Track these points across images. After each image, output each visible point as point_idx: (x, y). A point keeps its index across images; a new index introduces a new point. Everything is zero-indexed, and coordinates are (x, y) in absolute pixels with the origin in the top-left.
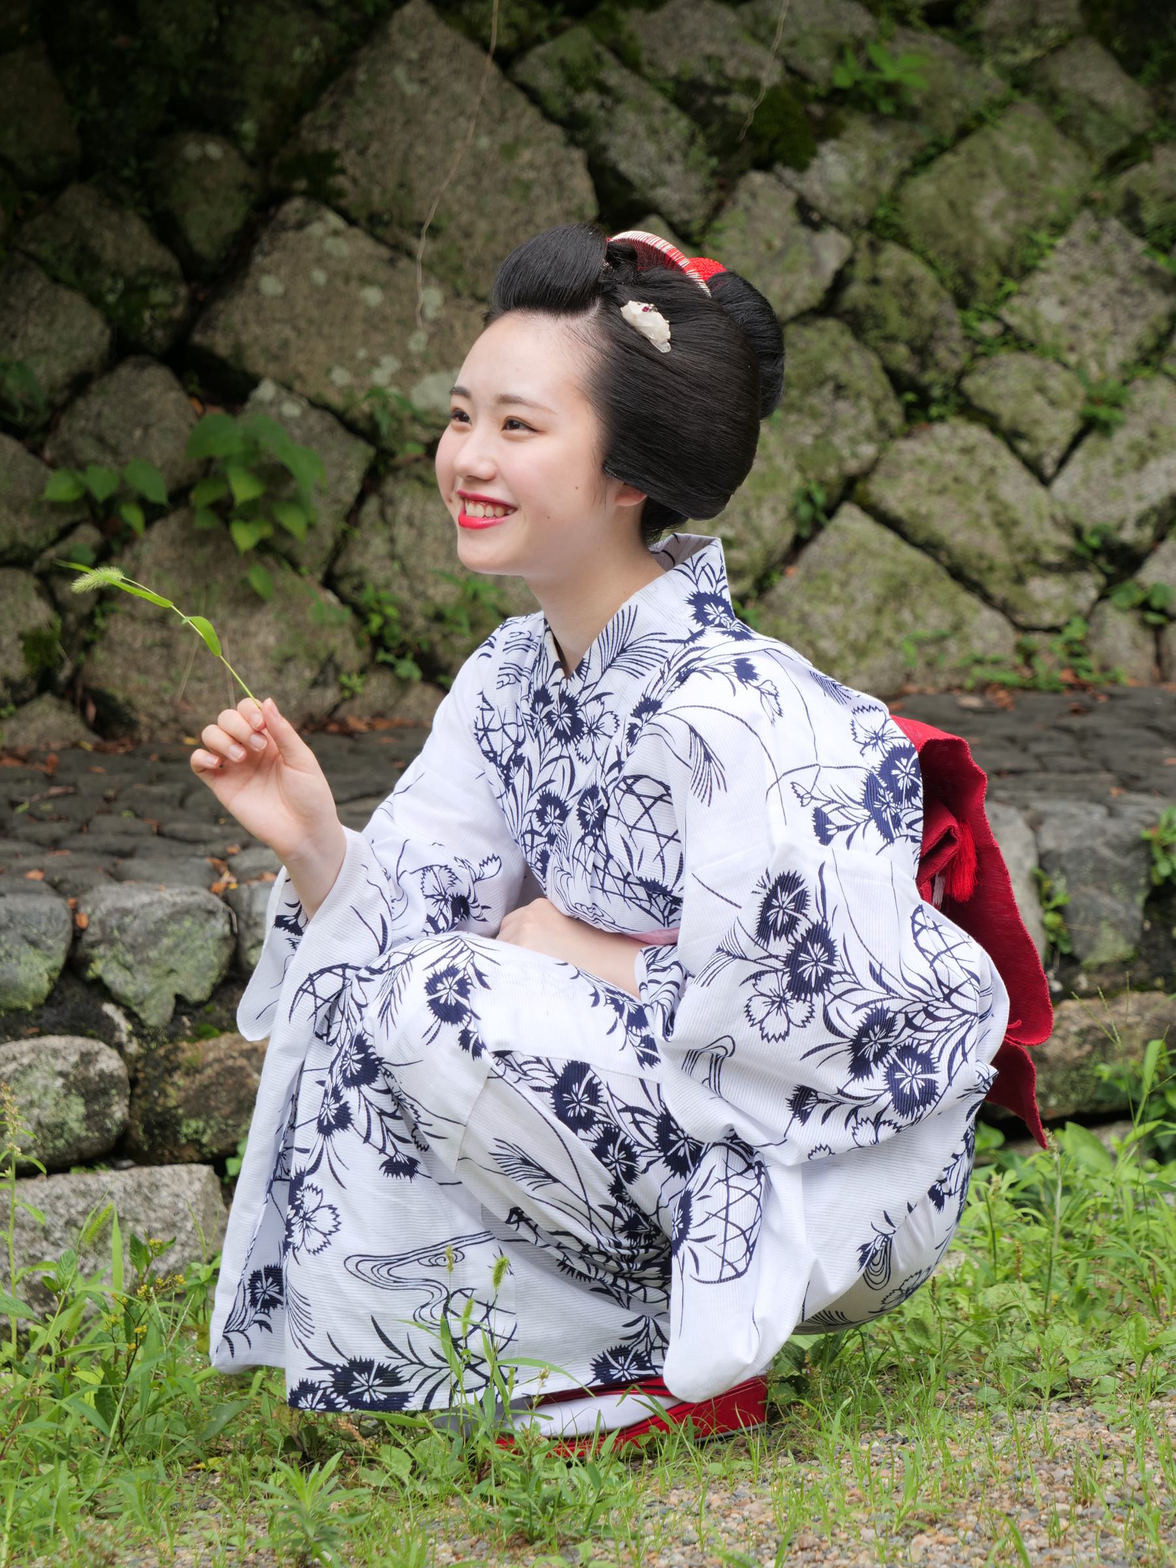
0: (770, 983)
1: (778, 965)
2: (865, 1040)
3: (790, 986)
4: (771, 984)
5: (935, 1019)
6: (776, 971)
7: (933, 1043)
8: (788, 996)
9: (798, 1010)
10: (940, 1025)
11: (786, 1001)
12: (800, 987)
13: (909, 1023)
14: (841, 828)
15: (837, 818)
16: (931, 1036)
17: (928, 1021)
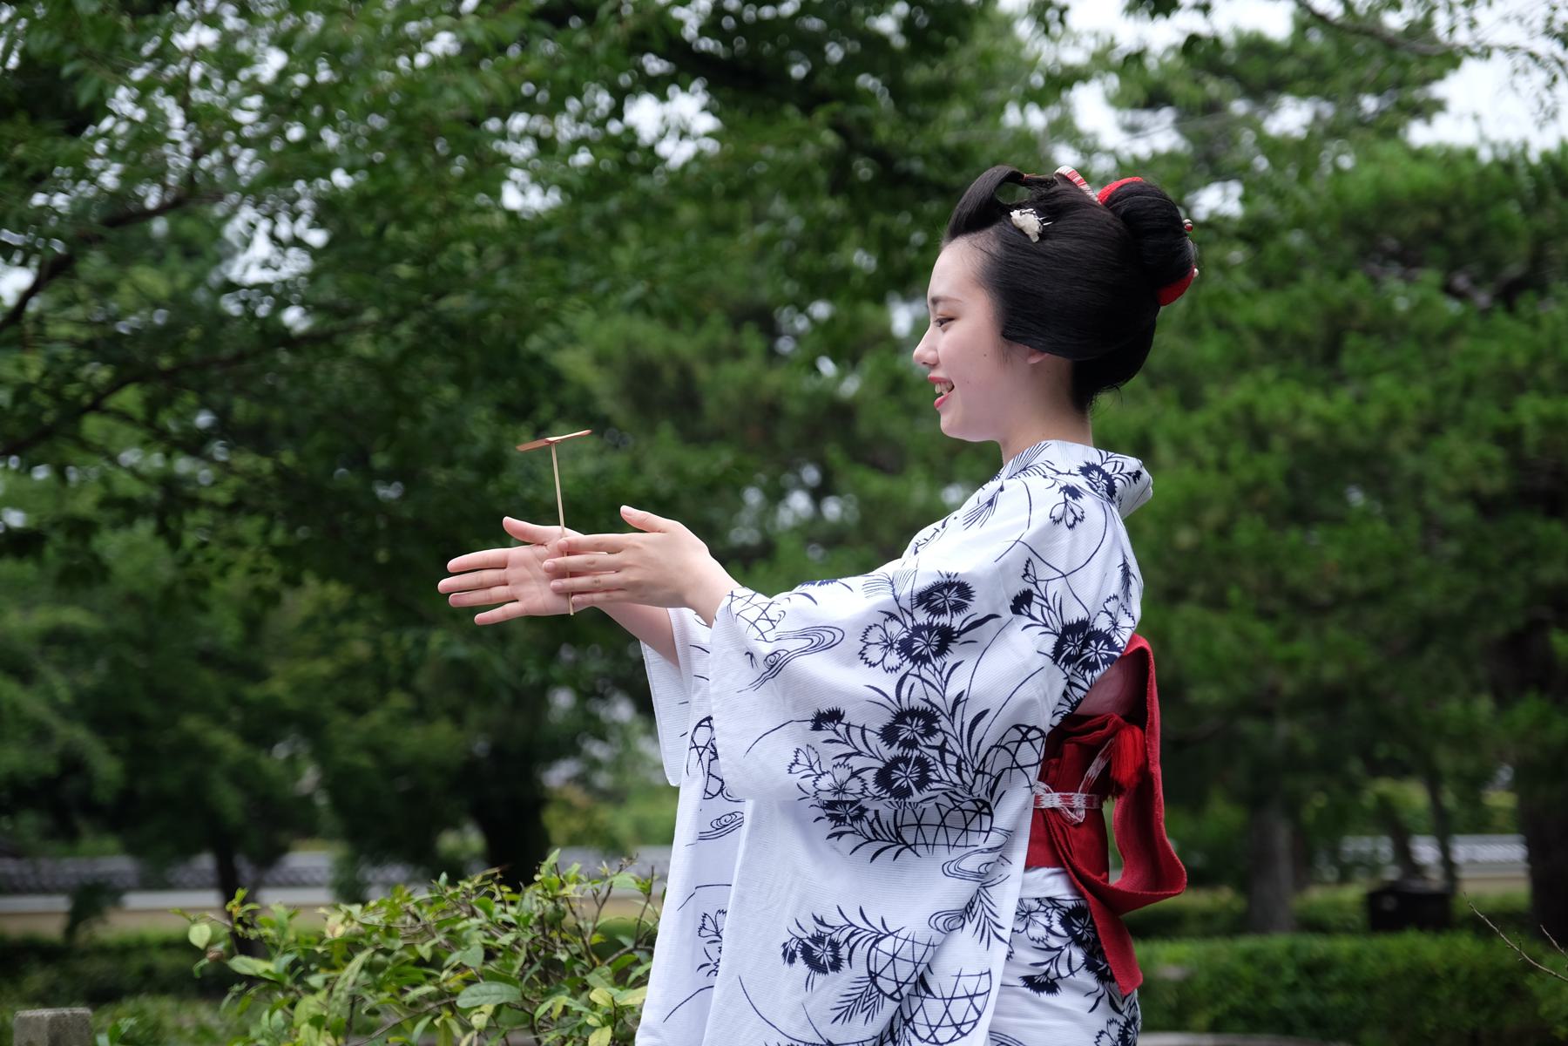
0: (895, 629)
1: (910, 625)
2: (908, 720)
3: (902, 642)
4: (895, 629)
5: (959, 773)
6: (905, 626)
7: (941, 780)
8: (896, 646)
9: (893, 659)
10: (956, 779)
11: (892, 648)
12: (906, 648)
13: (942, 749)
14: (1030, 616)
15: (1035, 610)
16: (944, 776)
17: (954, 769)
